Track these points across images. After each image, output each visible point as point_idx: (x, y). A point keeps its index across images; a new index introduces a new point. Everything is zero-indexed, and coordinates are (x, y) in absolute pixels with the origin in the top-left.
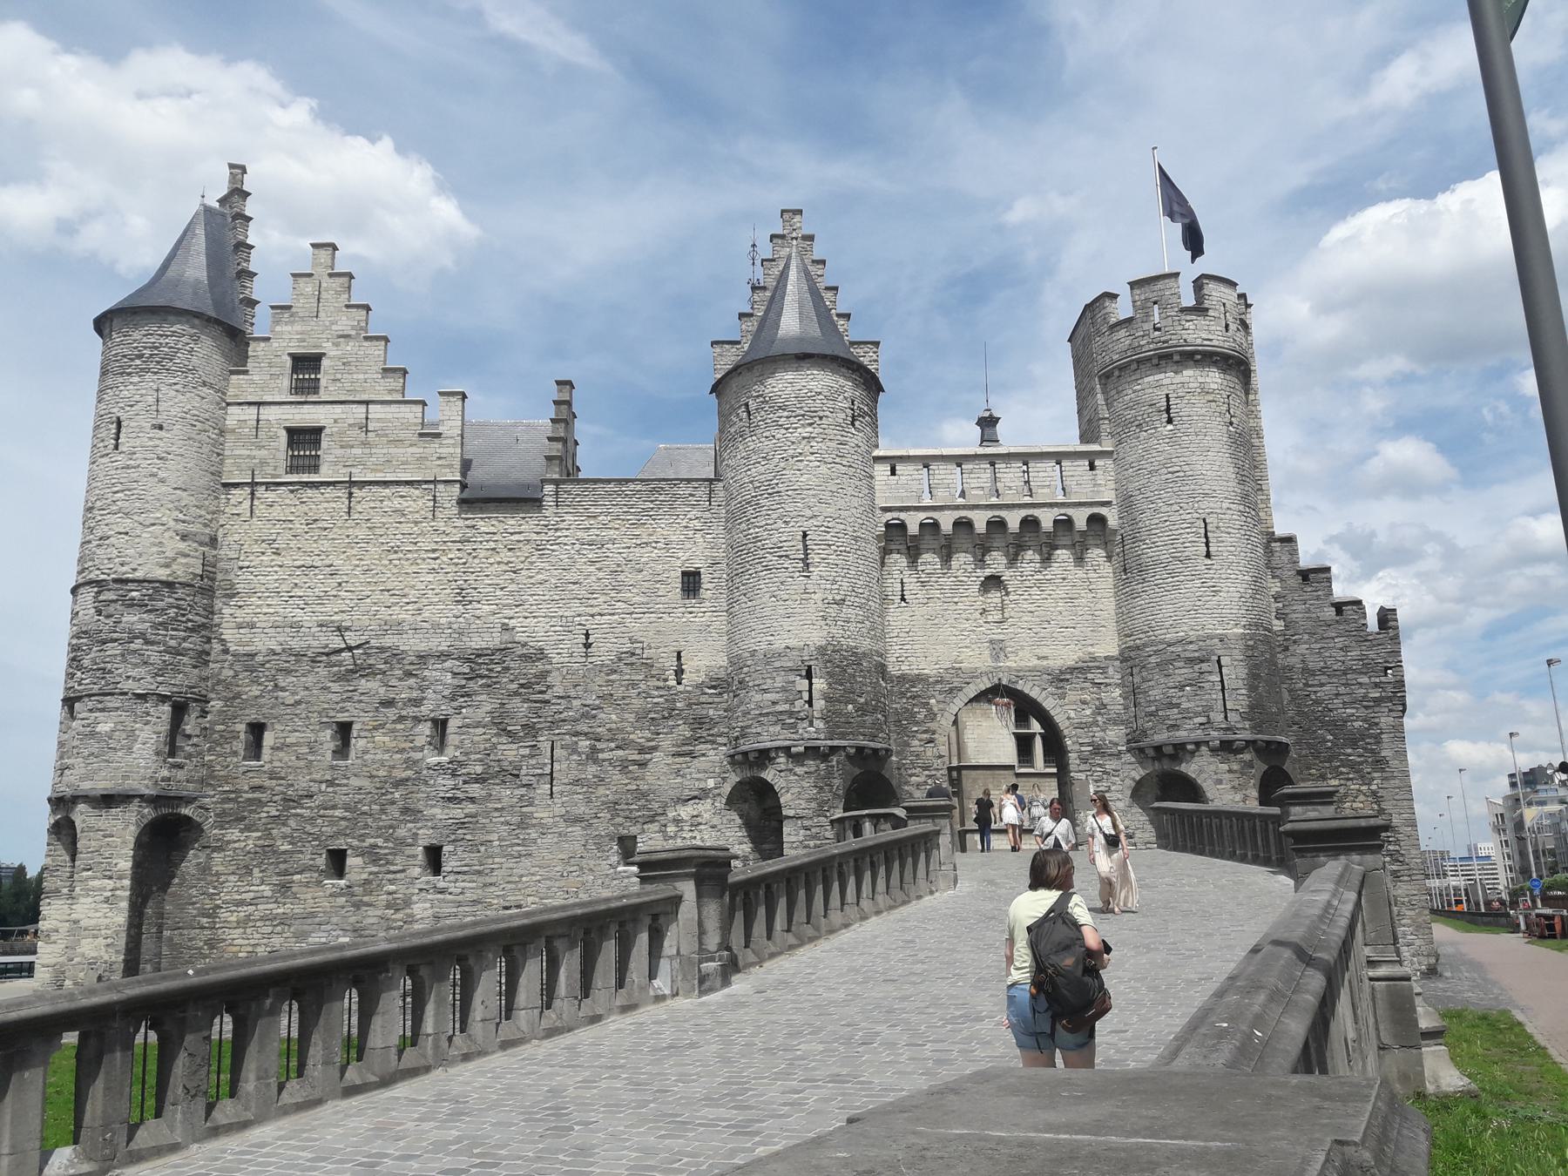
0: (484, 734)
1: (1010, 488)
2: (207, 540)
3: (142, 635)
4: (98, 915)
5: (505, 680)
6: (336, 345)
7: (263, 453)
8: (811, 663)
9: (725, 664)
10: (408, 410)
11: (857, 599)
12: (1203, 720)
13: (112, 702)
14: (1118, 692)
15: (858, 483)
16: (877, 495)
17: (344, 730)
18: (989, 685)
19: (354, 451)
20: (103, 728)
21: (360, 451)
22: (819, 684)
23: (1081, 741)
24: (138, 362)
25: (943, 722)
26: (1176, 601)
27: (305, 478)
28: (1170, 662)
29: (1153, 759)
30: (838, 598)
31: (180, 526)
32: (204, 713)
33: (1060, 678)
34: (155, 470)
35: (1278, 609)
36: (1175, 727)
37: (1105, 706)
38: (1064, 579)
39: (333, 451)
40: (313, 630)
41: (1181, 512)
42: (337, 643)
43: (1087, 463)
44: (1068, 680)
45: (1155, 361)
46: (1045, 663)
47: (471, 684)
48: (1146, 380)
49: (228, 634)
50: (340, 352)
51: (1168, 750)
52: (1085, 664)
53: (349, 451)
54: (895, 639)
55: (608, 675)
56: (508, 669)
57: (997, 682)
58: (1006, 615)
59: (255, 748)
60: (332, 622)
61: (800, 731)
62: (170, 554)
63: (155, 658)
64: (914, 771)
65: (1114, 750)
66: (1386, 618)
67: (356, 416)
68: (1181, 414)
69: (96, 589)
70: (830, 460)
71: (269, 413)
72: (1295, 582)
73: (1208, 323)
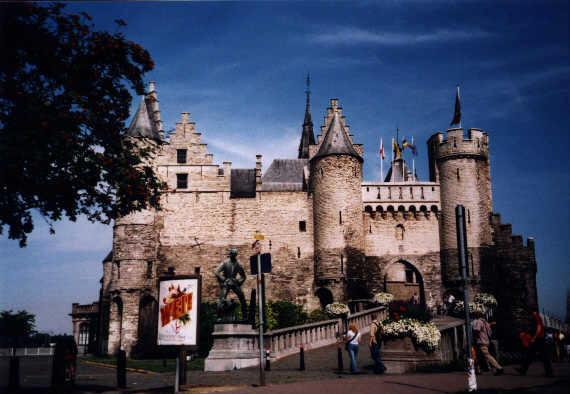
3: (139, 241)
19: (199, 182)
20: (129, 270)
22: (345, 260)
33: (422, 259)
42: (194, 243)
66: (530, 243)
71: (171, 169)
72: (499, 229)
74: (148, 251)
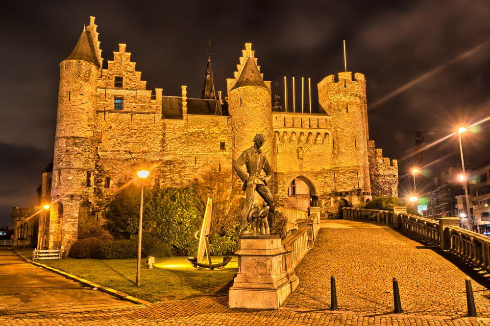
13: (72, 171)
19: (132, 104)
20: (70, 178)
21: (134, 104)
33: (317, 174)
42: (129, 156)
49: (99, 153)
56: (175, 166)
59: (107, 186)
63: (83, 158)
71: (110, 92)
74: (88, 162)
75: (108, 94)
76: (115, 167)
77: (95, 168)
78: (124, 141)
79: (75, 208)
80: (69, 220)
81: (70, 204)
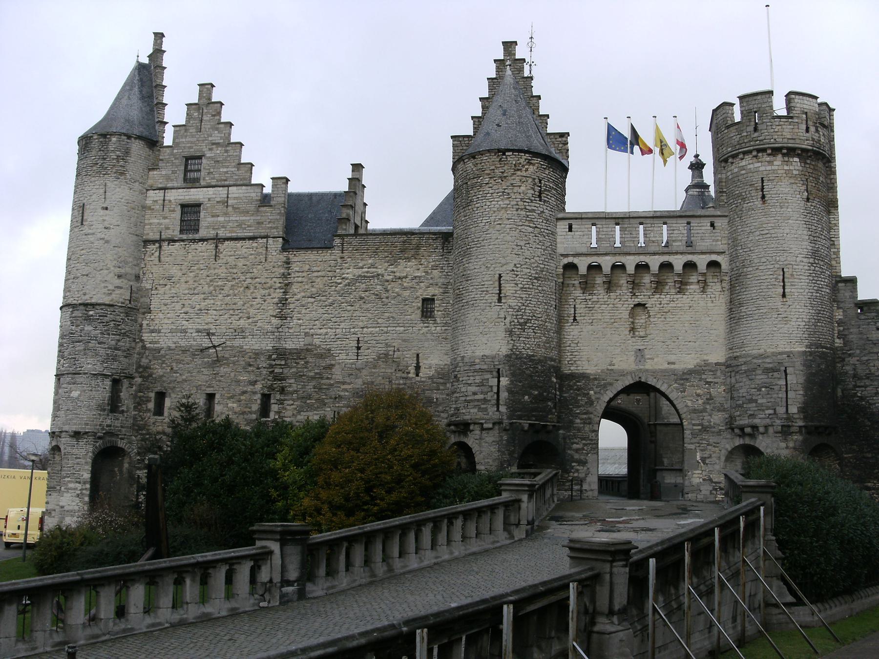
0: (292, 405)
1: (653, 242)
2: (133, 278)
4: (74, 504)
5: (305, 370)
6: (210, 149)
7: (167, 221)
8: (499, 367)
9: (448, 363)
10: (252, 191)
11: (536, 322)
12: (771, 412)
13: (79, 379)
14: (723, 388)
15: (541, 239)
16: (558, 245)
17: (211, 397)
18: (632, 382)
19: (221, 219)
20: (75, 394)
22: (504, 381)
23: (694, 422)
24: (95, 168)
25: (598, 407)
26: (760, 327)
27: (191, 236)
28: (754, 370)
29: (740, 436)
30: (522, 321)
31: (117, 270)
32: (131, 386)
33: (684, 377)
34: (103, 236)
35: (839, 331)
36: (752, 416)
37: (711, 398)
38: (690, 307)
39: (207, 219)
40: (193, 335)
41: (768, 263)
42: (206, 343)
43: (709, 224)
44: (687, 379)
45: (755, 153)
46: (672, 366)
47: (286, 371)
48: (749, 167)
49: (146, 336)
50: (213, 155)
51: (748, 430)
52: (700, 368)
53: (215, 219)
54: (568, 348)
55: (370, 368)
57: (638, 380)
58: (648, 332)
60: (205, 330)
61: (490, 413)
62: (111, 287)
64: (575, 440)
65: (715, 430)
67: (221, 196)
68: (771, 192)
69: (71, 310)
70: (521, 223)
71: (172, 195)
73: (792, 127)
74: (115, 359)
75: (170, 201)
76: (175, 369)
77: (137, 371)
78: (198, 306)
79: (83, 461)
80: (71, 485)
81: (75, 451)
